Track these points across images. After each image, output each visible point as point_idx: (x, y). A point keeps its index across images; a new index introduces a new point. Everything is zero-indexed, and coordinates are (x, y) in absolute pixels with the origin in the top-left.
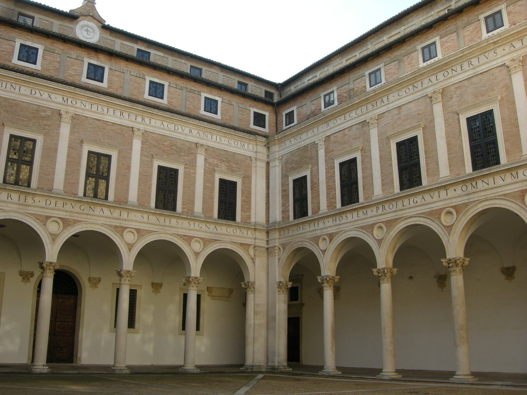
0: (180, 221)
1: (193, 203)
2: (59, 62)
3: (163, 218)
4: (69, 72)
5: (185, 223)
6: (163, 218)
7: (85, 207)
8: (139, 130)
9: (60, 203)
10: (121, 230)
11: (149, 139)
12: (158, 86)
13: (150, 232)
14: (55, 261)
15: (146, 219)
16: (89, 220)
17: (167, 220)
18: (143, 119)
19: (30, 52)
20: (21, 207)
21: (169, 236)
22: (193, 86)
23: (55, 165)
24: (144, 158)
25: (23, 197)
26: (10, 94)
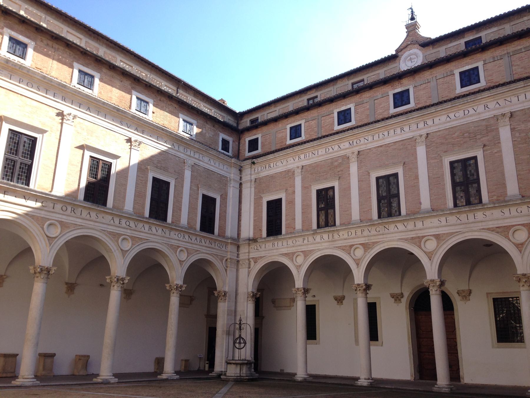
0: (488, 213)
1: (503, 185)
2: (368, 109)
3: (465, 215)
4: (378, 112)
5: (497, 213)
6: (465, 215)
7: (381, 228)
8: (421, 136)
9: (359, 231)
10: (418, 240)
11: (434, 140)
12: (472, 72)
13: (451, 235)
14: (363, 282)
15: (444, 223)
16: (385, 239)
17: (471, 216)
18: (425, 123)
19: (346, 115)
21: (476, 233)
22: (517, 46)
23: (351, 201)
24: (432, 161)
26: (312, 160)
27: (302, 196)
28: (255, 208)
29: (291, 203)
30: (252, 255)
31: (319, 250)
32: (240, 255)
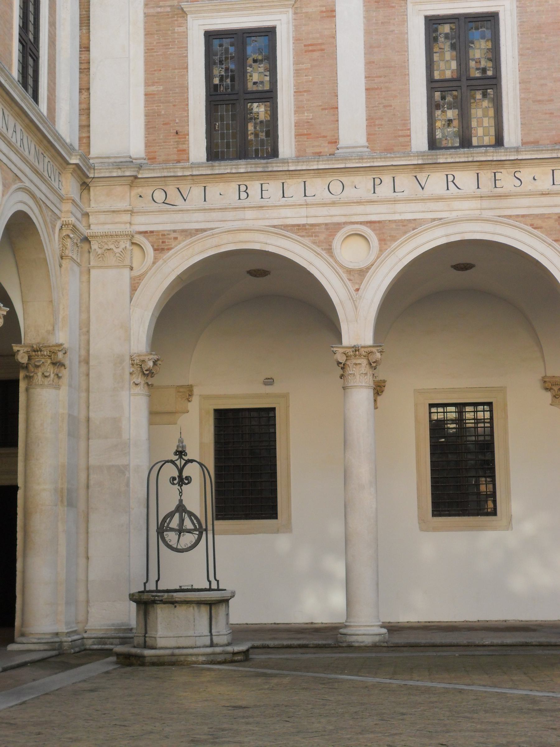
20: (486, 203)
25: (486, 176)
27: (367, 33)
28: (149, 50)
29: (319, 50)
30: (142, 223)
31: (442, 222)
32: (92, 219)
